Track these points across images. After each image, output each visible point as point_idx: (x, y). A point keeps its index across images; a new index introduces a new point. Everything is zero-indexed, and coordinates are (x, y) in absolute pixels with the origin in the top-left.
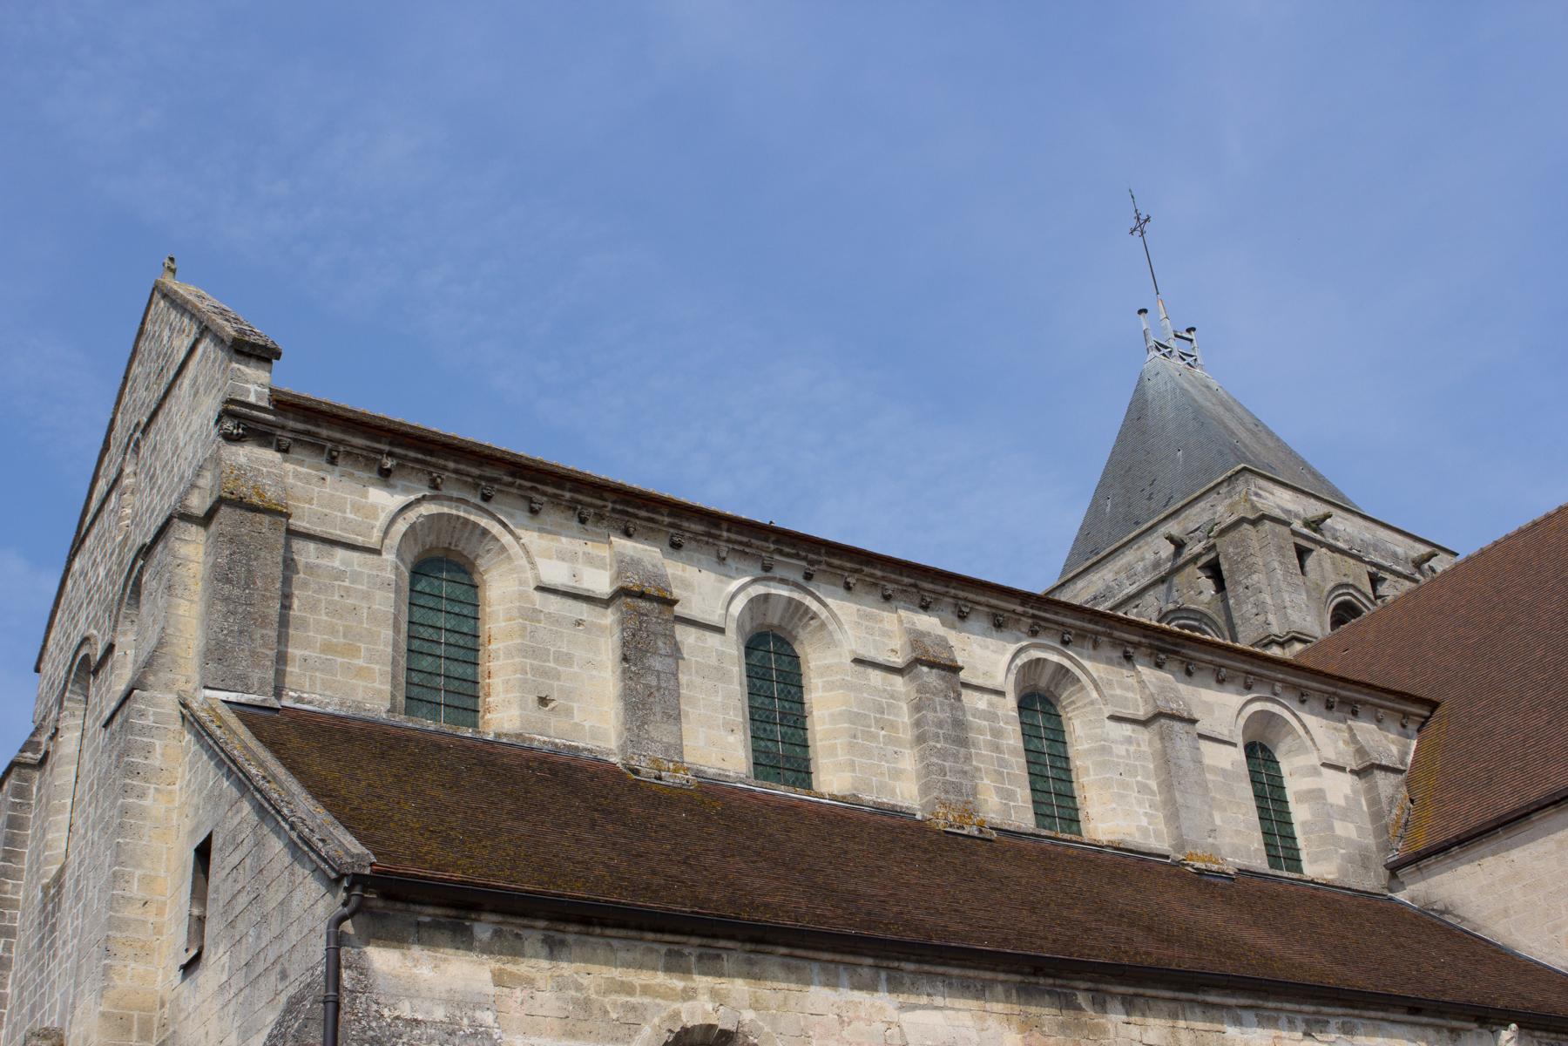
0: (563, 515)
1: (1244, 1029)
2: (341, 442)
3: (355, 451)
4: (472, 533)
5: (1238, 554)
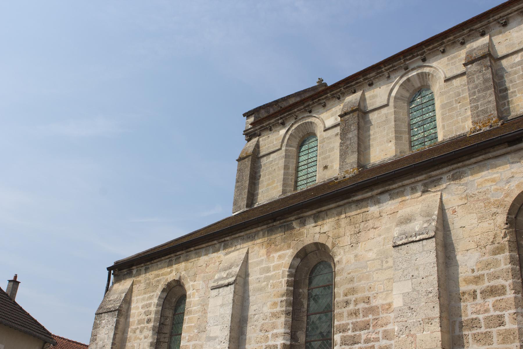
0: (333, 101)
1: (381, 204)
2: (269, 124)
3: (274, 123)
4: (309, 125)
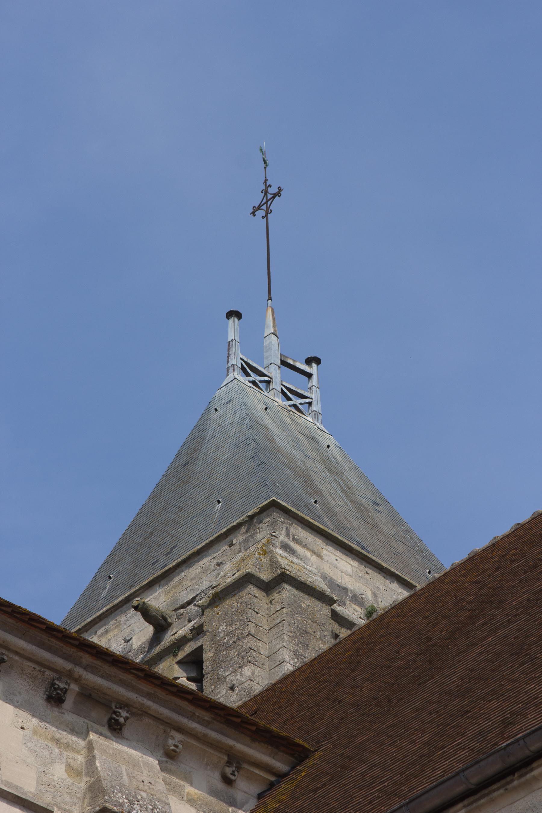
5: (232, 633)
